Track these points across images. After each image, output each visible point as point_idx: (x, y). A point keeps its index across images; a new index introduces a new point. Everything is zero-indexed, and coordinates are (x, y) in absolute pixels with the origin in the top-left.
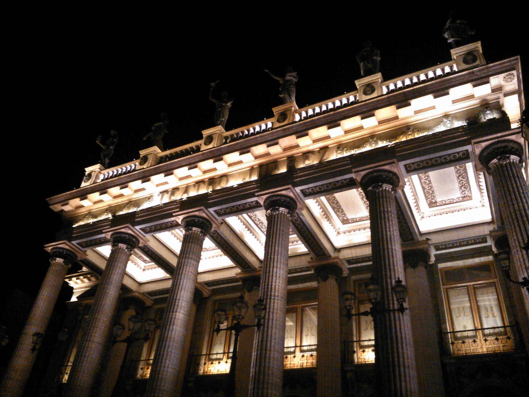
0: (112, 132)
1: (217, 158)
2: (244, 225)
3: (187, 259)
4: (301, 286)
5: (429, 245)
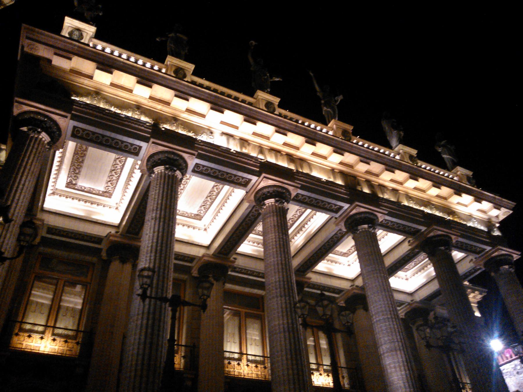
1: (310, 140)
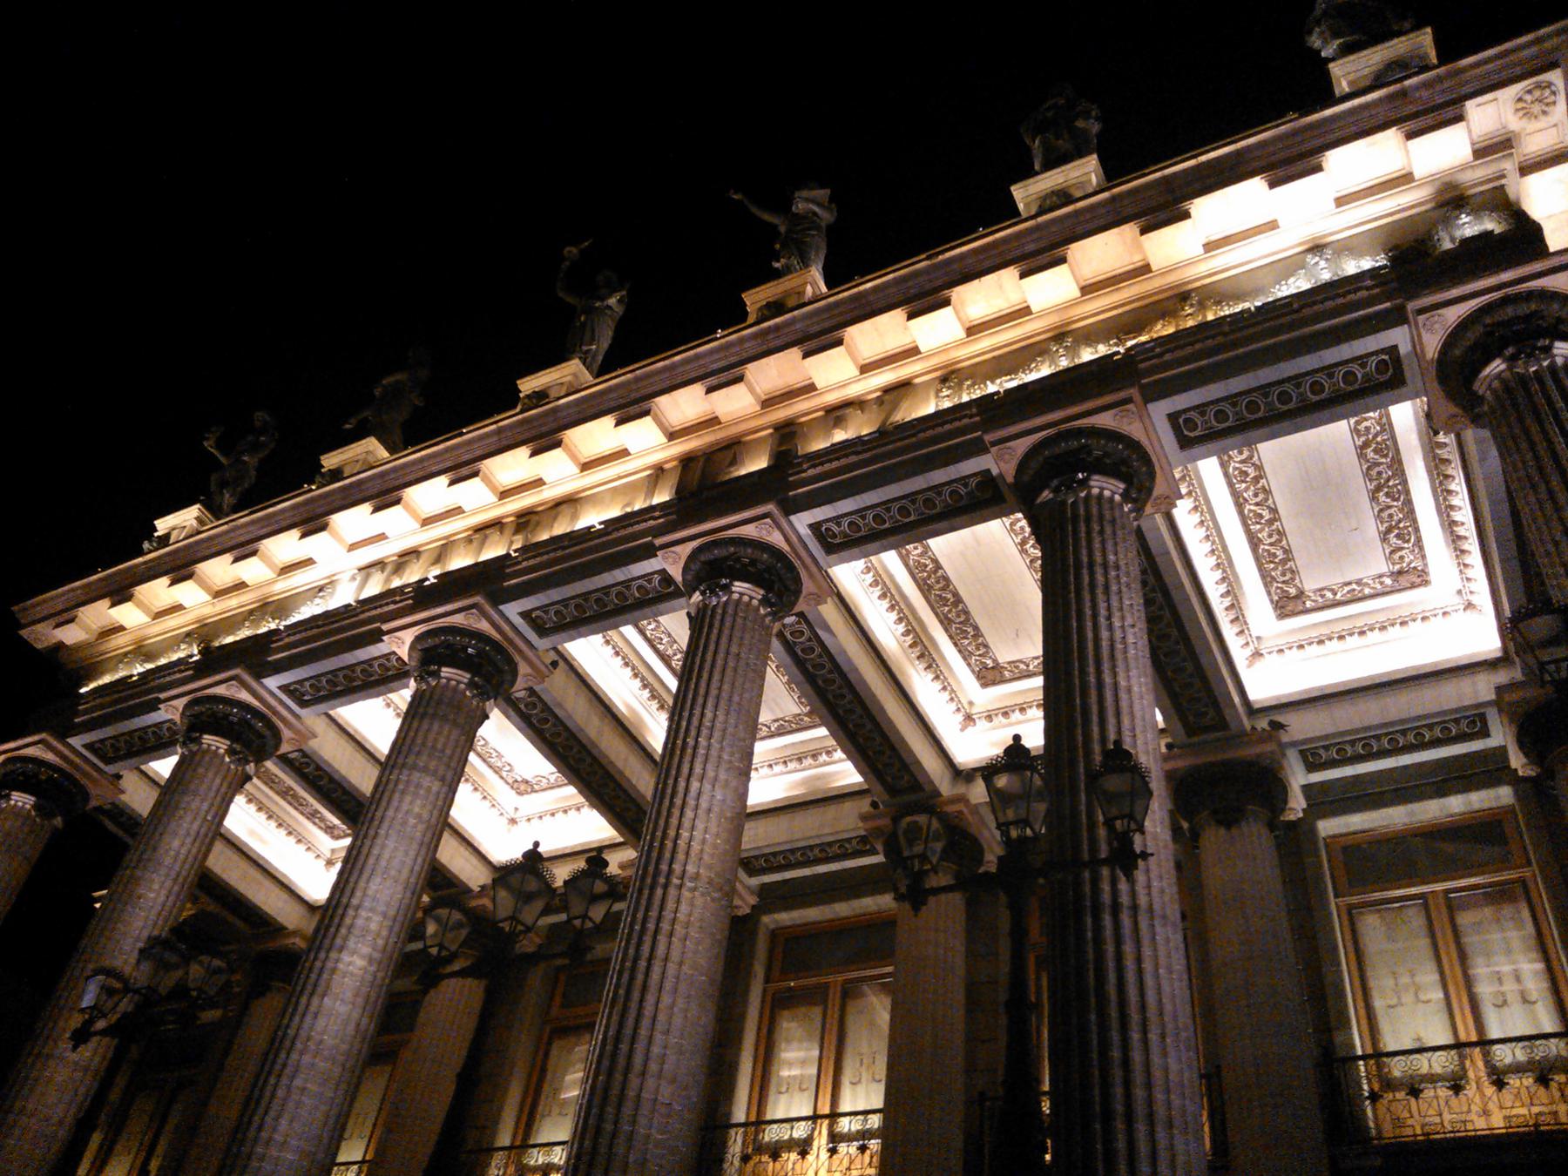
0: (260, 416)
2: (645, 686)
3: (406, 772)
4: (842, 909)
5: (1283, 746)
